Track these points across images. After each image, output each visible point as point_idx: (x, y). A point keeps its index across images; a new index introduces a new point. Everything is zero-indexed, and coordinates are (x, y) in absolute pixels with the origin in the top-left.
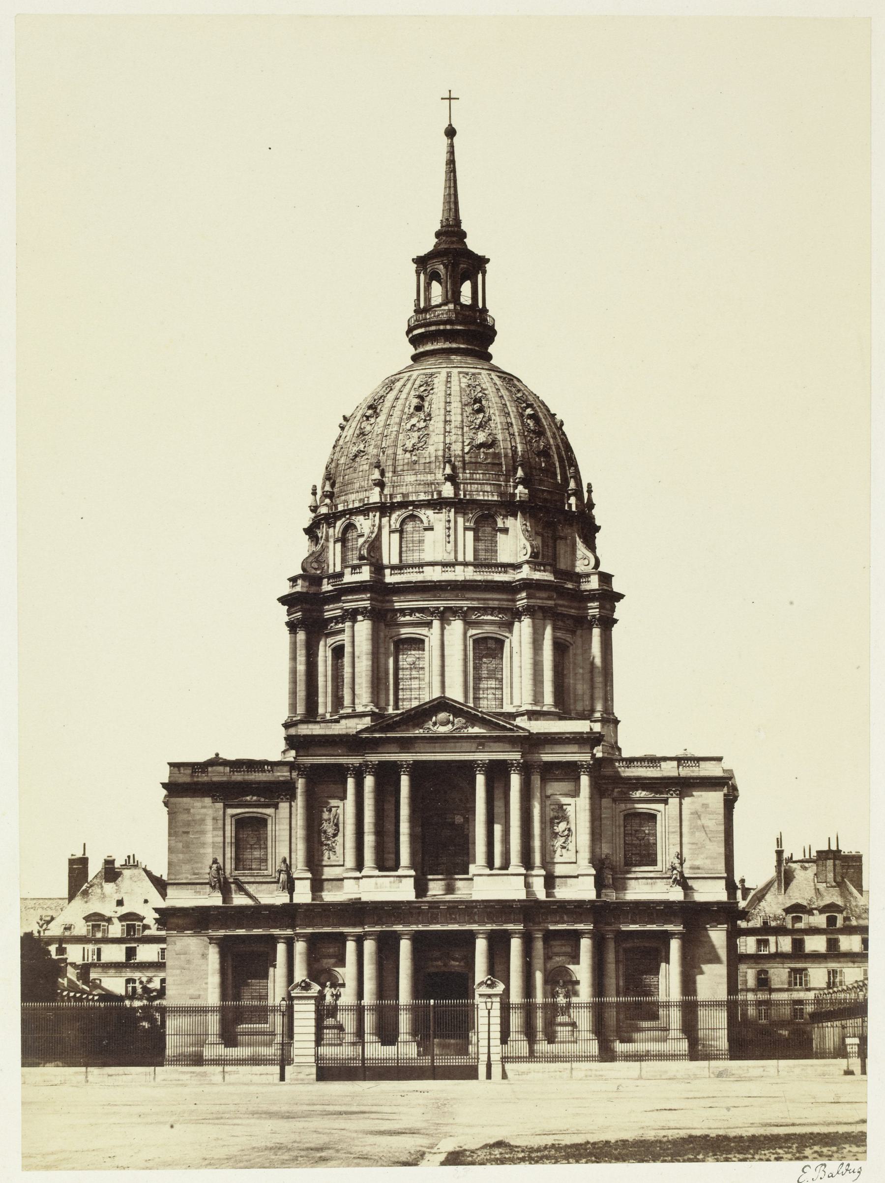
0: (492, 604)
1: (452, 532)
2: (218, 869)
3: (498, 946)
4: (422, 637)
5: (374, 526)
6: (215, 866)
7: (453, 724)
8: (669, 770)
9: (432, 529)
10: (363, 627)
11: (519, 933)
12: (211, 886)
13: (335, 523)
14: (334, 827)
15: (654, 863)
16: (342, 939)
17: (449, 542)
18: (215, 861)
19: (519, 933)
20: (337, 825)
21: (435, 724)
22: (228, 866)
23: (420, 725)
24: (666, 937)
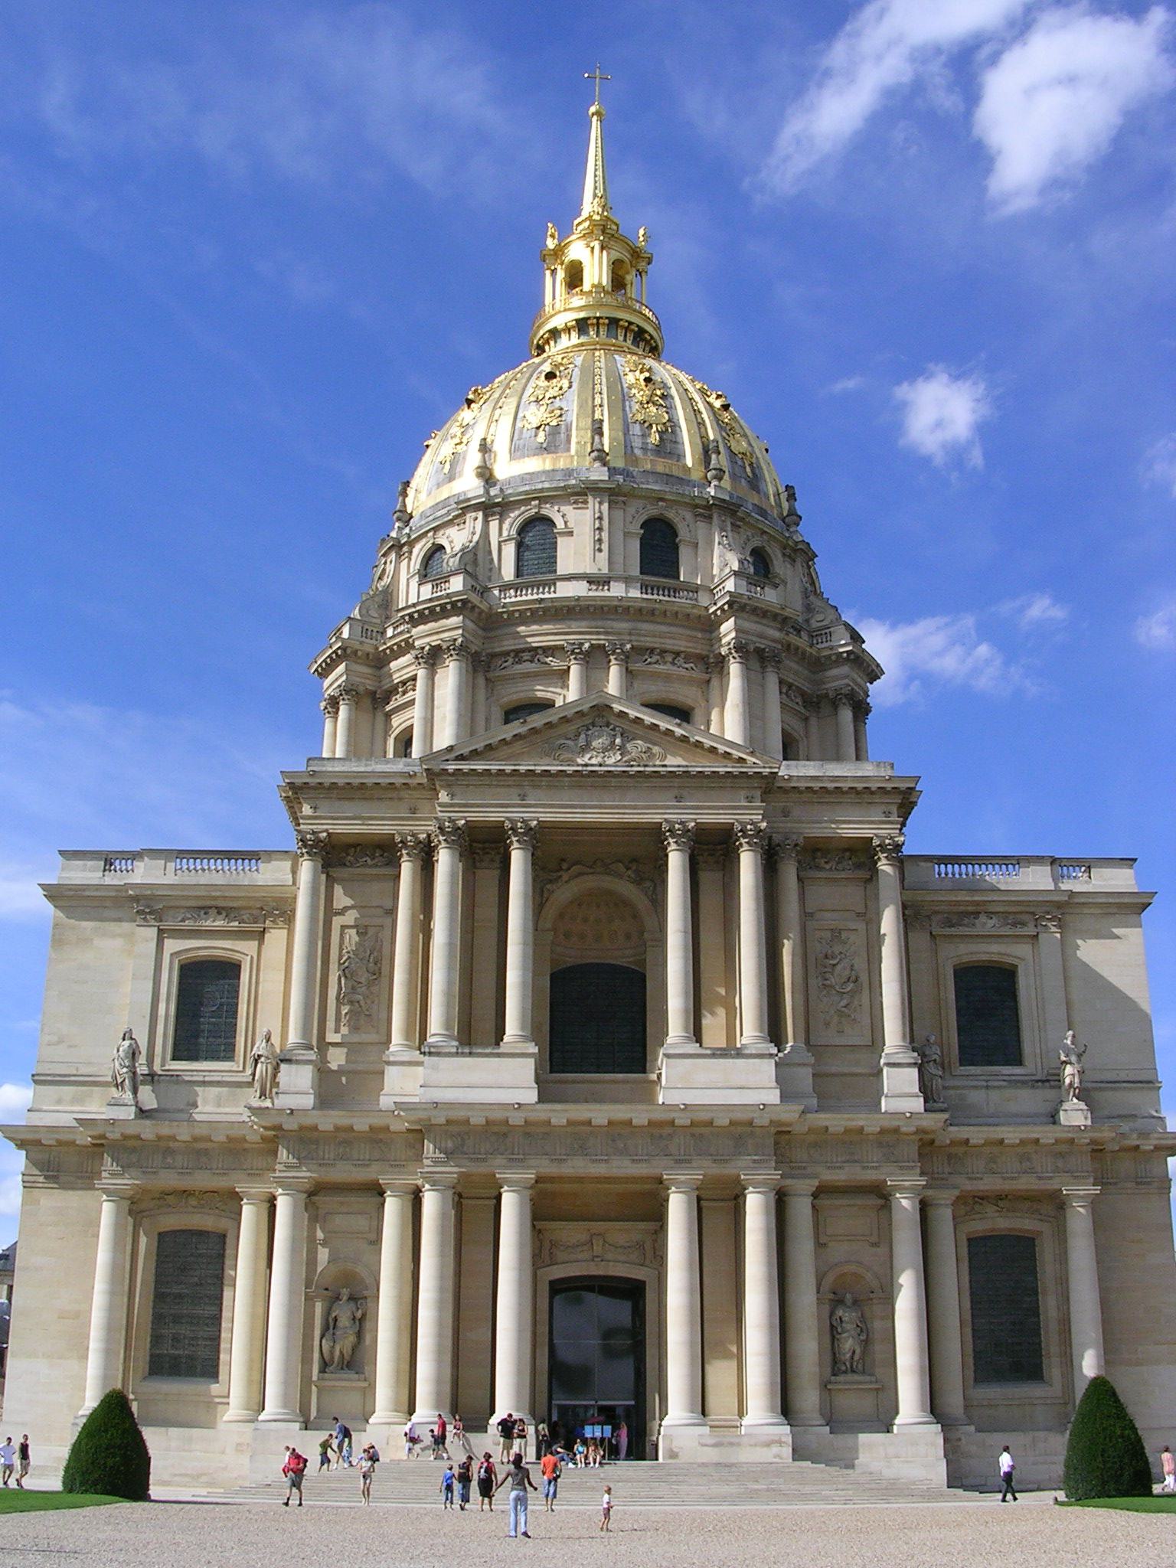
0: (669, 644)
1: (605, 535)
2: (133, 1054)
3: (719, 1210)
5: (474, 533)
6: (127, 1043)
7: (622, 748)
8: (1036, 880)
9: (571, 534)
10: (449, 676)
11: (764, 1183)
12: (117, 1086)
13: (411, 552)
17: (600, 550)
18: (128, 1035)
19: (764, 1183)
22: (158, 1049)
23: (553, 751)
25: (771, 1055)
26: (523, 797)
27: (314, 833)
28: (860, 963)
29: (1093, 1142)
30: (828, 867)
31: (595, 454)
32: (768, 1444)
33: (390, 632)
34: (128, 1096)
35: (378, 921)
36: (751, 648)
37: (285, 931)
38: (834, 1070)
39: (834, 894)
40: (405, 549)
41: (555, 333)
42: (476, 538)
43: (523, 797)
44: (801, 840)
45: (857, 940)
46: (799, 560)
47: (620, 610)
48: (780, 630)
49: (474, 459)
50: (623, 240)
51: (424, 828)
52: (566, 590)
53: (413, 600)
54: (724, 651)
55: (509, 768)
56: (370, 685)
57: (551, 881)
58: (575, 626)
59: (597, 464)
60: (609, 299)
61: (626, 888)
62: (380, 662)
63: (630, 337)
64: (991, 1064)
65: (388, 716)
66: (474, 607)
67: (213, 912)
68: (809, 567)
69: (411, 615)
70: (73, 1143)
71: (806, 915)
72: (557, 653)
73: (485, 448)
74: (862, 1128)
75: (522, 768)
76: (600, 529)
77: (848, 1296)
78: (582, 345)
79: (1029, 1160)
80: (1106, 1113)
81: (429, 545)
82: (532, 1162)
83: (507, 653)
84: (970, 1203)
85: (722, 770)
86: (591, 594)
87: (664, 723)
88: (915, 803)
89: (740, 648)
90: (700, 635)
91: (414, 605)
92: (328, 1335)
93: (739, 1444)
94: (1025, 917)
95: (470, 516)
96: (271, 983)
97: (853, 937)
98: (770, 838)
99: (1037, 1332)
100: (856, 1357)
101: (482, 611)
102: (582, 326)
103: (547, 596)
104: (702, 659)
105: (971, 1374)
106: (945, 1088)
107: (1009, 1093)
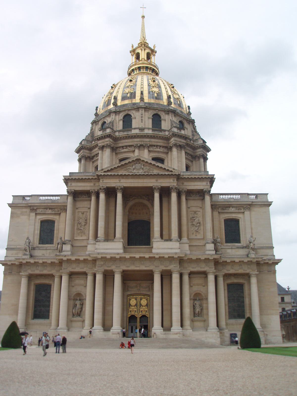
0: (159, 144)
2: (29, 243)
4: (130, 157)
6: (27, 240)
7: (143, 169)
13: (98, 123)
14: (85, 221)
15: (238, 241)
16: (85, 274)
17: (142, 122)
18: (28, 238)
19: (176, 271)
20: (86, 220)
21: (134, 169)
22: (35, 242)
24: (248, 276)
25: (178, 241)
26: (120, 181)
27: (71, 190)
28: (201, 219)
29: (257, 261)
30: (193, 196)
31: (141, 99)
32: (177, 334)
33: (93, 142)
34: (28, 253)
35: (86, 211)
36: (178, 145)
37: (65, 213)
38: (194, 244)
39: (195, 203)
40: (97, 123)
41: (133, 70)
42: (113, 120)
43: (120, 181)
44: (186, 190)
45: (200, 214)
46: (191, 124)
47: (147, 136)
48: (185, 140)
49: (113, 101)
50: (150, 48)
51: (96, 189)
52: (134, 132)
53: (99, 134)
54: (171, 145)
55: (116, 174)
56: (89, 155)
57: (128, 201)
58: (136, 140)
59: (142, 101)
60: (146, 62)
61: (146, 202)
62: (91, 149)
63: (151, 71)
64: (232, 242)
65: (93, 162)
66: (112, 136)
67: (48, 209)
68: (193, 125)
69: (97, 138)
70: (15, 264)
71: (188, 208)
72: (132, 147)
73: (115, 98)
74: (200, 258)
75: (120, 174)
76: (142, 117)
77: (198, 298)
78: (139, 73)
79: (241, 266)
80: (260, 254)
81: (102, 122)
82: (122, 267)
83: (120, 147)
84: (227, 276)
85: (167, 173)
86: (140, 132)
87: (153, 162)
88: (214, 181)
89: (176, 145)
90: (166, 142)
91: (98, 136)
92: (75, 309)
93: (170, 334)
94: (241, 208)
95: (112, 114)
96: (62, 226)
97: (199, 213)
98: (179, 190)
99: (243, 306)
100: (199, 313)
101: (114, 137)
102: (139, 68)
103: (130, 133)
104: (166, 147)
105: (227, 317)
106: (221, 249)
107: (237, 250)
